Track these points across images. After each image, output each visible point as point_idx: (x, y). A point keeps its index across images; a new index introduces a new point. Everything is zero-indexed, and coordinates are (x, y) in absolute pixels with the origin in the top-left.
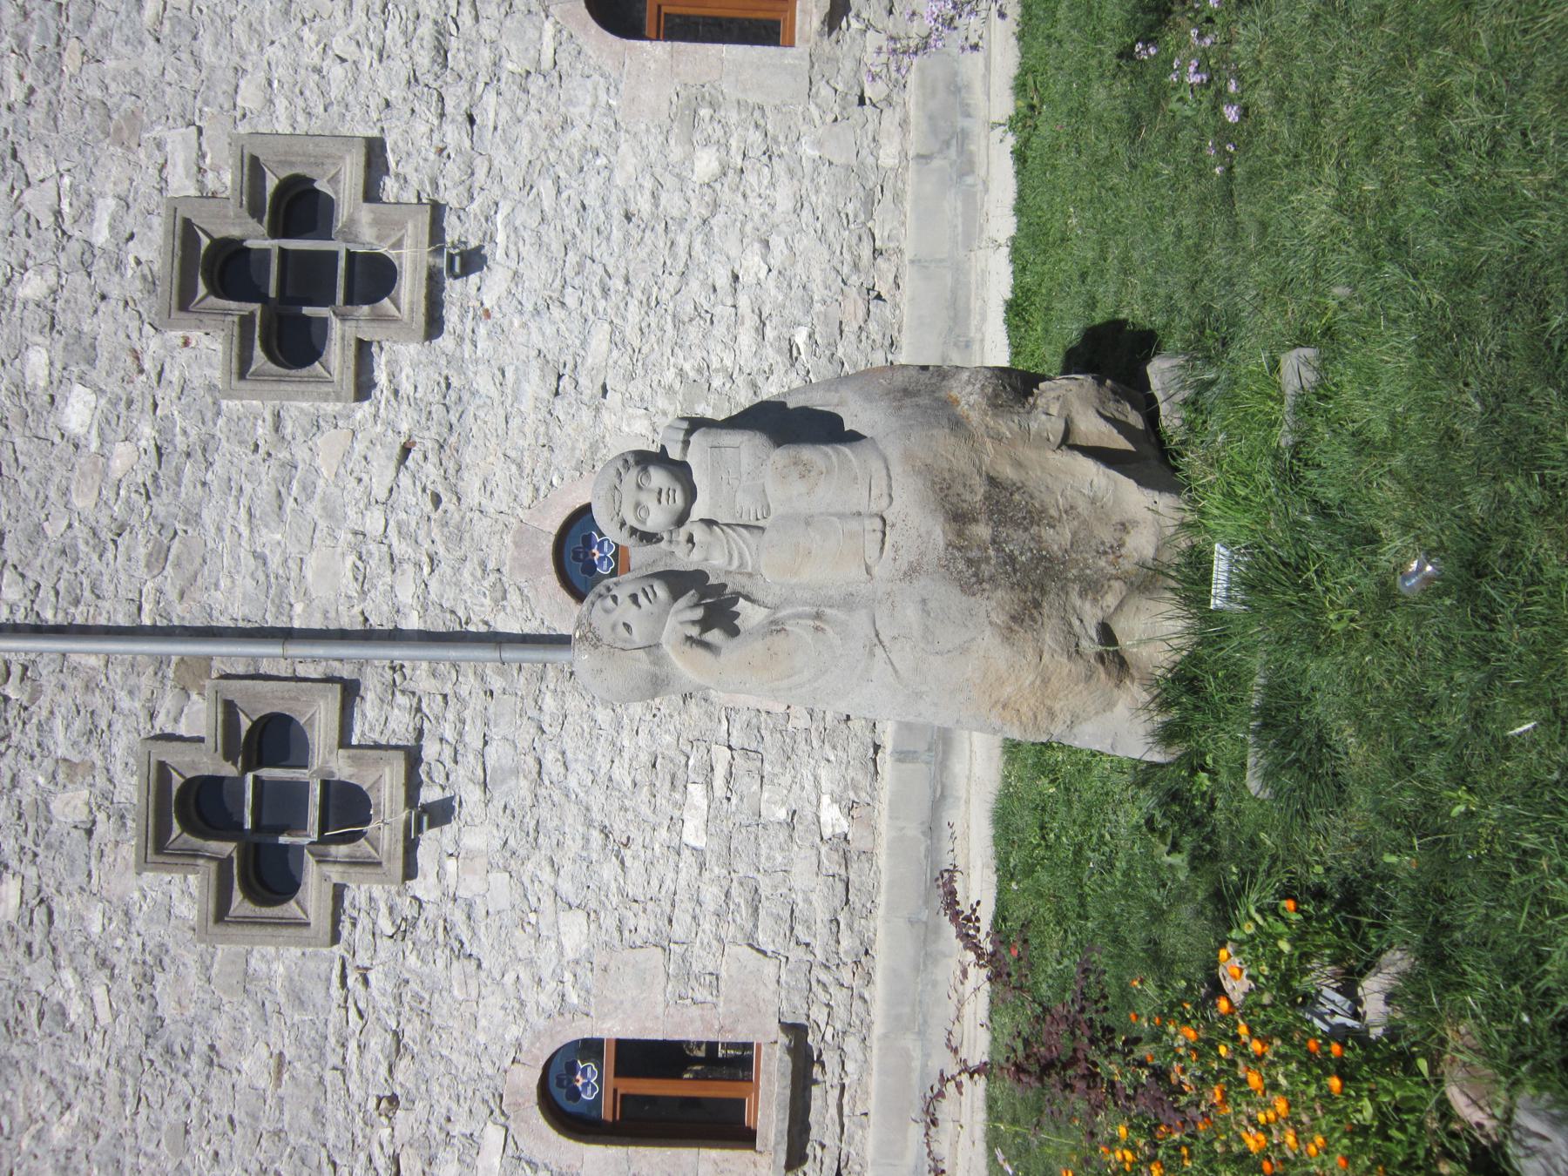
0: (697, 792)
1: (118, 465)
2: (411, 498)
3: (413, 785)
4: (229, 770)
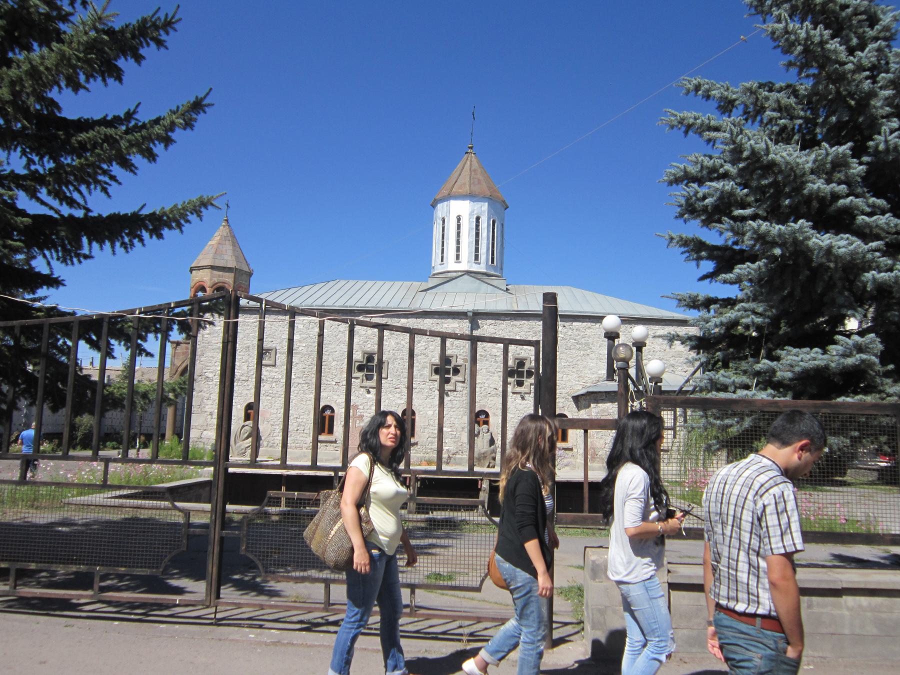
0: (450, 430)
1: (494, 350)
2: (489, 390)
3: (450, 391)
4: (452, 365)
